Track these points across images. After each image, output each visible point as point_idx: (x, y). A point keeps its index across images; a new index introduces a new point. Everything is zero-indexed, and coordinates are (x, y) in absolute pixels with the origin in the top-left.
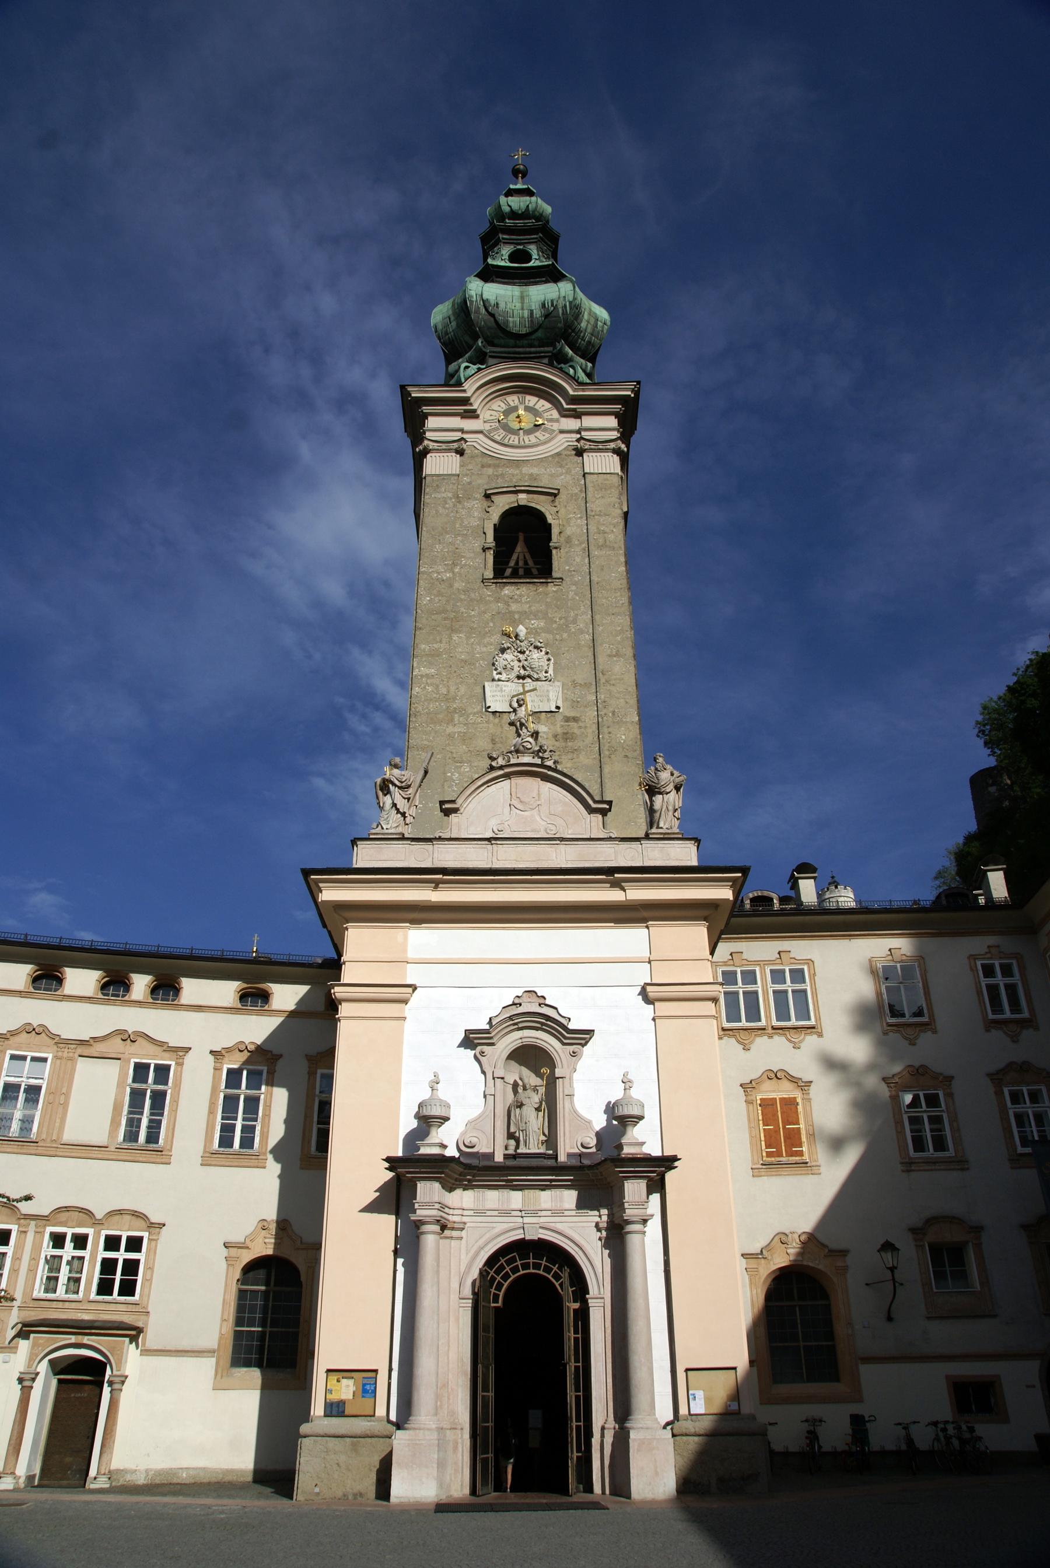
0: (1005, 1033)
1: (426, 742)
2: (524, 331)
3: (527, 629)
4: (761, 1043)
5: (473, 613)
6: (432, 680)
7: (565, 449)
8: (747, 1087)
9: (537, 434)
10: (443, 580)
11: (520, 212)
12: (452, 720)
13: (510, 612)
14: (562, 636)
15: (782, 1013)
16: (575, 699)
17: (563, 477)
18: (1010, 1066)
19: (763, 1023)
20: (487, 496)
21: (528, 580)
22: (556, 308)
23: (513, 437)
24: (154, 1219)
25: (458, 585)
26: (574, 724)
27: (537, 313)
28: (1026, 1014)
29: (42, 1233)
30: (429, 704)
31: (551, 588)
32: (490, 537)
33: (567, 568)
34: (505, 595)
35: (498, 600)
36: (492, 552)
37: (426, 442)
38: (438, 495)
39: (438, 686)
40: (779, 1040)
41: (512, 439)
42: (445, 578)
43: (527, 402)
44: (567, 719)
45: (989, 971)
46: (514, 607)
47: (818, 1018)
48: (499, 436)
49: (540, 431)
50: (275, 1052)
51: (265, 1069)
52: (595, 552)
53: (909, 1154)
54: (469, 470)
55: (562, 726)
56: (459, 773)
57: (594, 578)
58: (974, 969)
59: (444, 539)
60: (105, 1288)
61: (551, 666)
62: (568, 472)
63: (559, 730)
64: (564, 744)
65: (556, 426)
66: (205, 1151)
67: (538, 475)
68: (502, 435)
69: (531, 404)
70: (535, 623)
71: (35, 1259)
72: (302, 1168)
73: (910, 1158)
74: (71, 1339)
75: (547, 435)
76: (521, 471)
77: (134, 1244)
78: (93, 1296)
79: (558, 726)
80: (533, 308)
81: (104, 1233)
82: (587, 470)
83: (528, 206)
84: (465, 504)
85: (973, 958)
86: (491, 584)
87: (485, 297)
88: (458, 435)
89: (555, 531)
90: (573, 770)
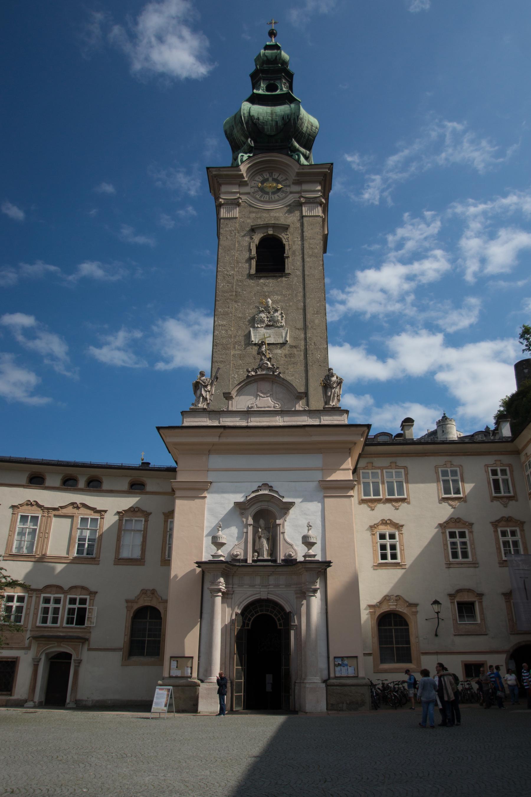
0: (500, 502)
1: (221, 359)
2: (273, 133)
3: (272, 300)
4: (380, 507)
5: (245, 292)
6: (225, 327)
7: (293, 202)
8: (372, 528)
9: (279, 194)
10: (230, 276)
11: (272, 60)
12: (234, 348)
13: (264, 292)
14: (289, 304)
15: (391, 492)
16: (295, 337)
17: (291, 218)
18: (502, 519)
19: (381, 497)
21: (273, 275)
22: (290, 120)
23: (266, 196)
24: (93, 589)
26: (295, 349)
27: (280, 123)
28: (512, 494)
29: (40, 597)
30: (223, 340)
32: (254, 252)
33: (293, 268)
34: (261, 282)
35: (258, 285)
36: (255, 260)
37: (220, 200)
38: (227, 229)
39: (227, 330)
40: (388, 505)
41: (265, 197)
42: (231, 274)
43: (273, 176)
44: (292, 347)
45: (494, 473)
46: (266, 289)
47: (408, 495)
48: (259, 195)
49: (280, 192)
50: (148, 512)
51: (143, 519)
52: (307, 259)
53: (449, 559)
54: (243, 215)
55: (289, 350)
56: (238, 375)
57: (306, 273)
58: (487, 472)
59: (230, 253)
60: (70, 621)
61: (284, 320)
63: (287, 352)
64: (289, 359)
65: (288, 189)
66: (115, 558)
67: (279, 217)
68: (260, 195)
69: (276, 177)
70: (276, 297)
71: (36, 609)
72: (161, 565)
73: (450, 562)
74: (54, 644)
75: (284, 195)
76: (270, 215)
77: (83, 601)
78: (65, 625)
79: (287, 350)
80: (278, 120)
81: (69, 596)
82: (304, 214)
83: (276, 57)
84: (241, 234)
85: (487, 466)
86: (254, 277)
87: (251, 114)
89: (287, 248)
90: (294, 372)
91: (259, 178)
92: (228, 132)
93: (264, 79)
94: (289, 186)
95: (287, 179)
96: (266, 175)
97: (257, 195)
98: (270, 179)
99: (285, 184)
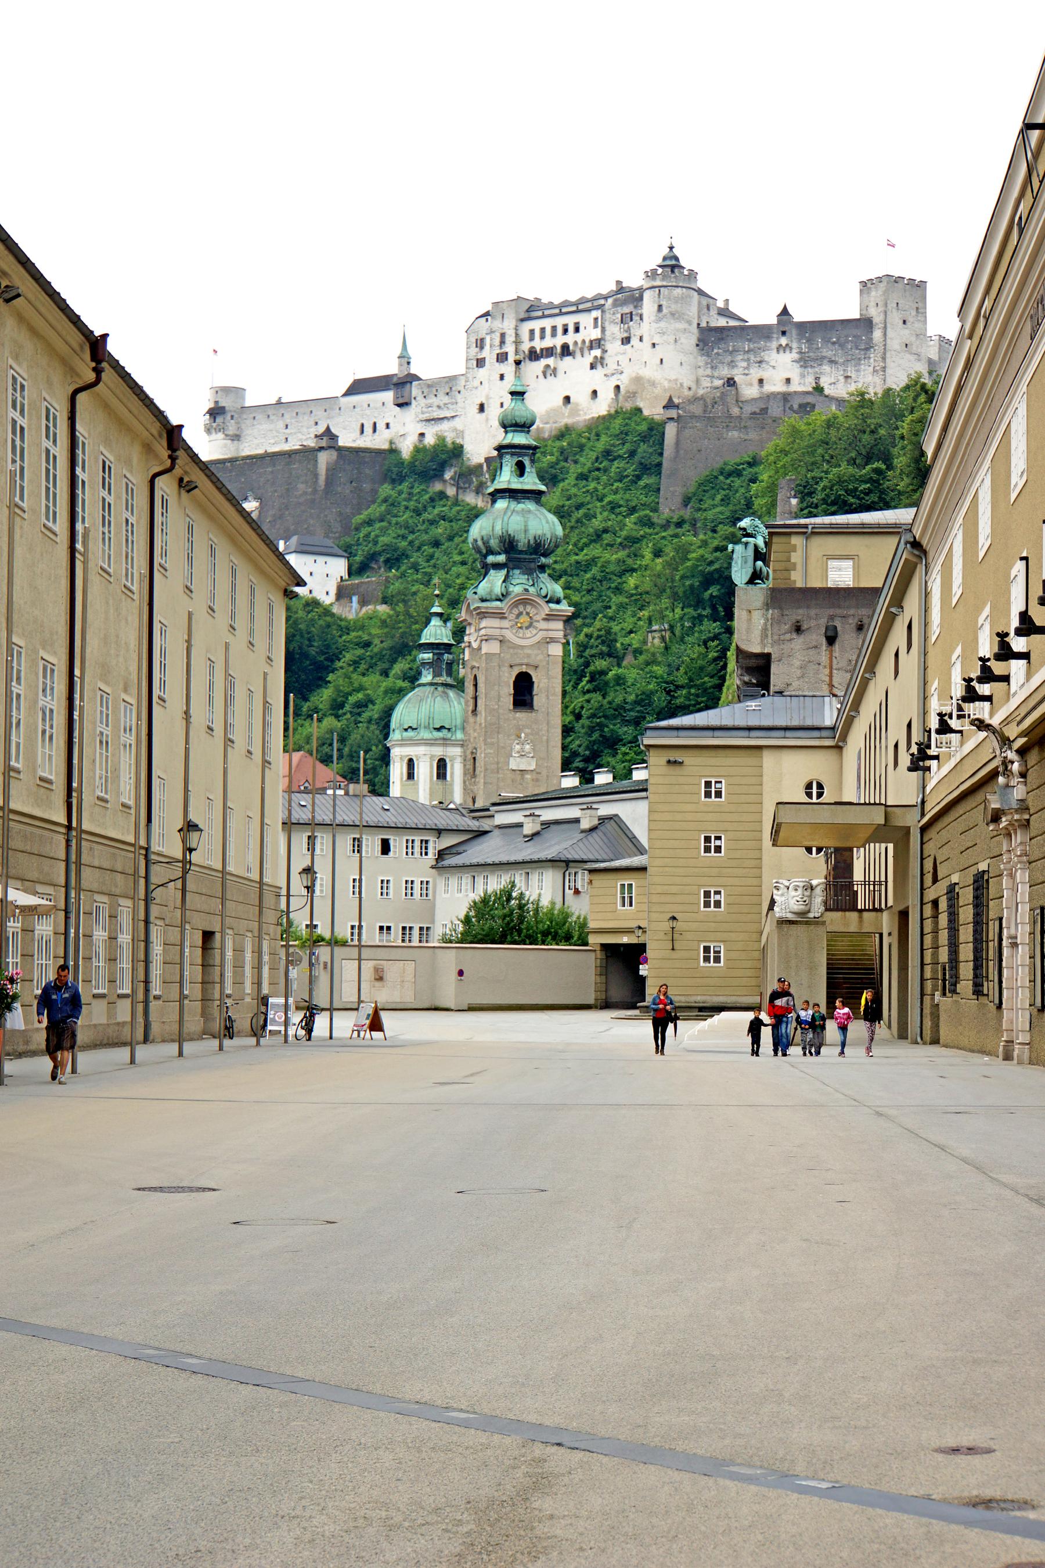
20: (511, 666)
25: (501, 711)
27: (532, 542)
31: (534, 714)
35: (514, 719)
44: (538, 773)
57: (550, 710)
62: (542, 653)
63: (534, 777)
70: (527, 730)
88: (497, 632)
89: (535, 686)
92: (485, 539)
93: (513, 454)
94: (538, 621)
95: (537, 614)
96: (521, 608)
98: (524, 613)
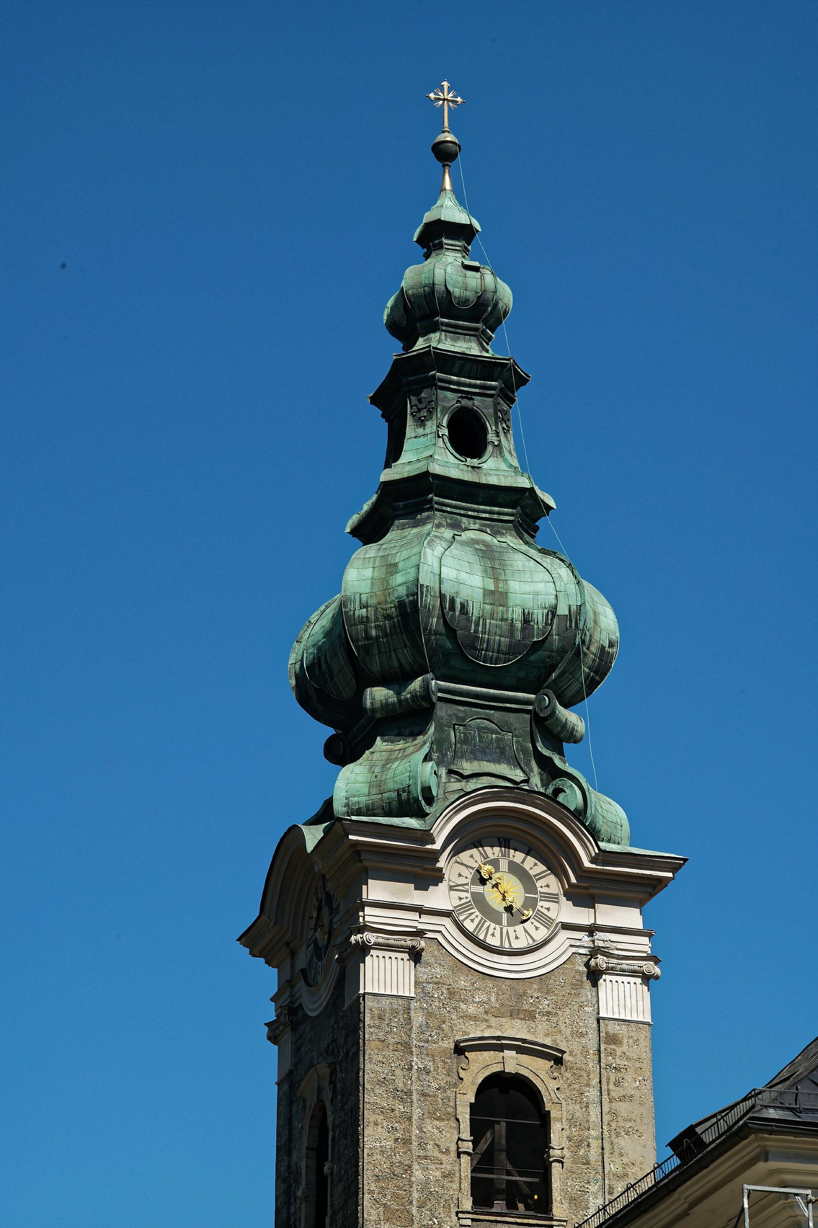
23: (493, 925)
32: (466, 1134)
41: (491, 931)
48: (472, 921)
91: (472, 856)
97: (468, 920)
99: (545, 890)
